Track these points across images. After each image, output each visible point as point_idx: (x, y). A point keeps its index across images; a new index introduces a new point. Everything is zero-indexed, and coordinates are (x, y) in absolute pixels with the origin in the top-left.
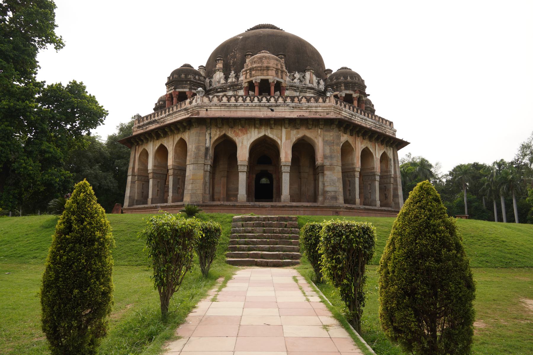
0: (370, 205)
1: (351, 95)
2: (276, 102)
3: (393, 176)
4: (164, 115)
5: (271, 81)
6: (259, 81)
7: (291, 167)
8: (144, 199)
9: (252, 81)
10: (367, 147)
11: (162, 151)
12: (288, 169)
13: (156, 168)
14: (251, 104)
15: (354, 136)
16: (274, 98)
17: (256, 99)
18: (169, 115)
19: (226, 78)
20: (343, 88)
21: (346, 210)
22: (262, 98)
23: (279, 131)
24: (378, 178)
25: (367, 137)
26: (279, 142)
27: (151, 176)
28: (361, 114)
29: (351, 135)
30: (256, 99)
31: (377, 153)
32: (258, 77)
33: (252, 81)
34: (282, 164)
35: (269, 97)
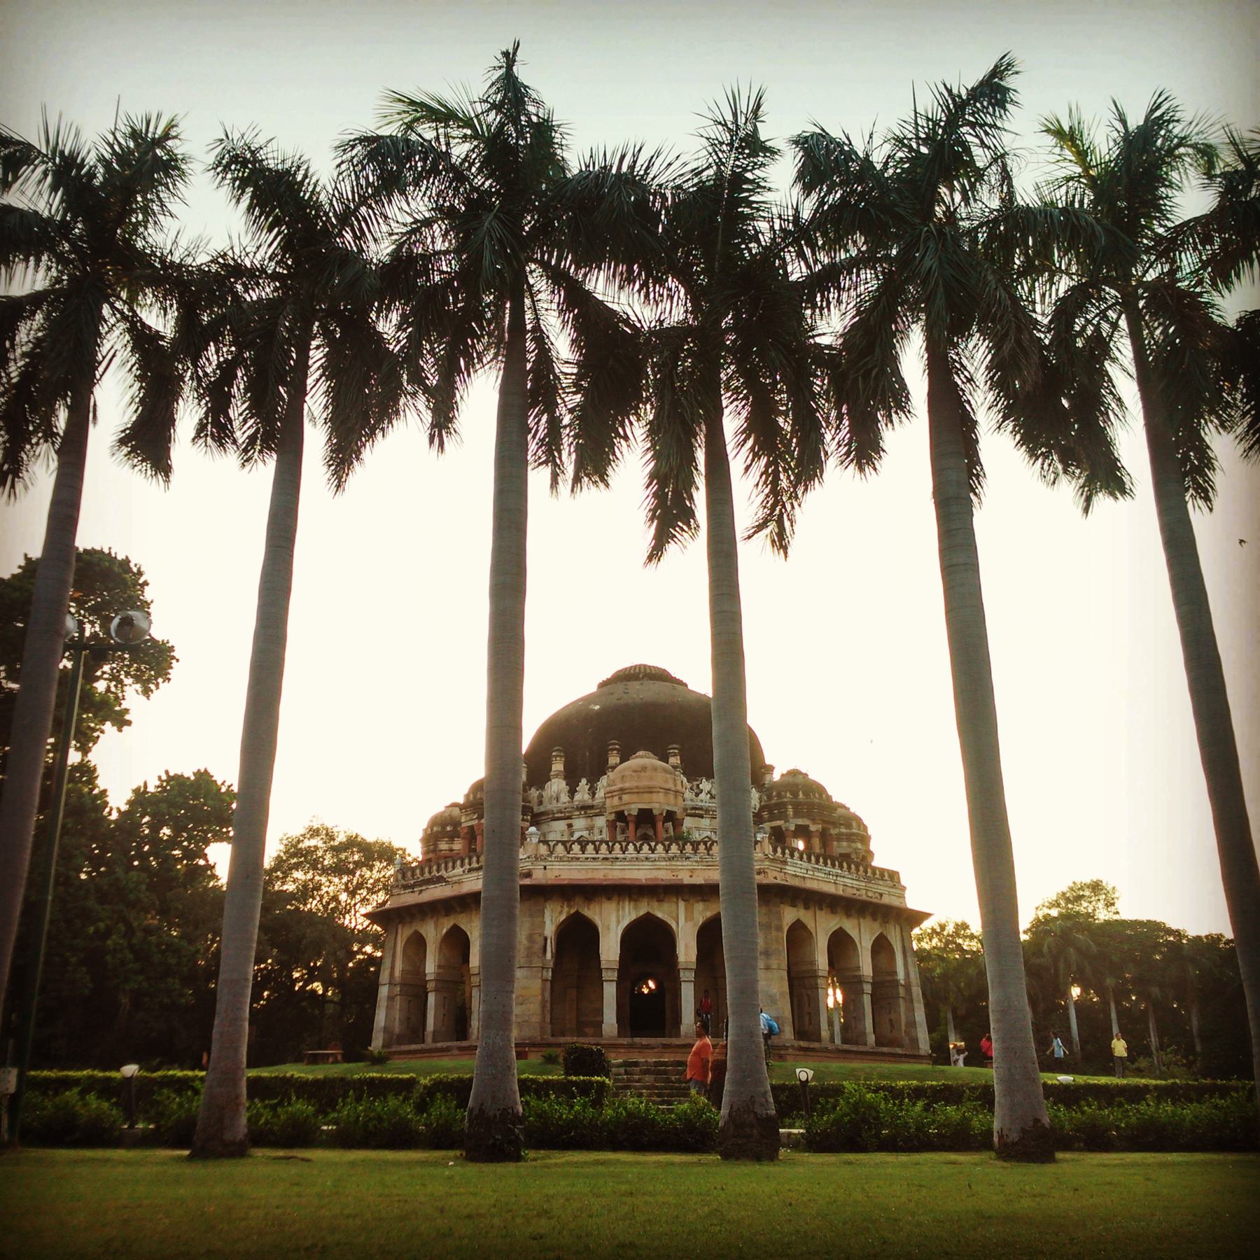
0: (857, 1044)
1: (807, 826)
2: (667, 852)
3: (902, 982)
4: (459, 870)
5: (656, 812)
6: (635, 813)
7: (698, 972)
8: (414, 1029)
9: (623, 811)
10: (841, 928)
11: (457, 942)
12: (691, 976)
13: (440, 971)
14: (623, 856)
15: (812, 909)
16: (663, 845)
17: (631, 847)
18: (470, 870)
19: (572, 792)
20: (790, 812)
21: (798, 1053)
22: (642, 845)
23: (674, 906)
24: (868, 988)
25: (839, 910)
26: (674, 926)
27: (431, 986)
28: (826, 864)
29: (807, 907)
30: (631, 847)
31: (863, 935)
32: (633, 806)
33: (623, 811)
34: (680, 967)
35: (653, 844)
